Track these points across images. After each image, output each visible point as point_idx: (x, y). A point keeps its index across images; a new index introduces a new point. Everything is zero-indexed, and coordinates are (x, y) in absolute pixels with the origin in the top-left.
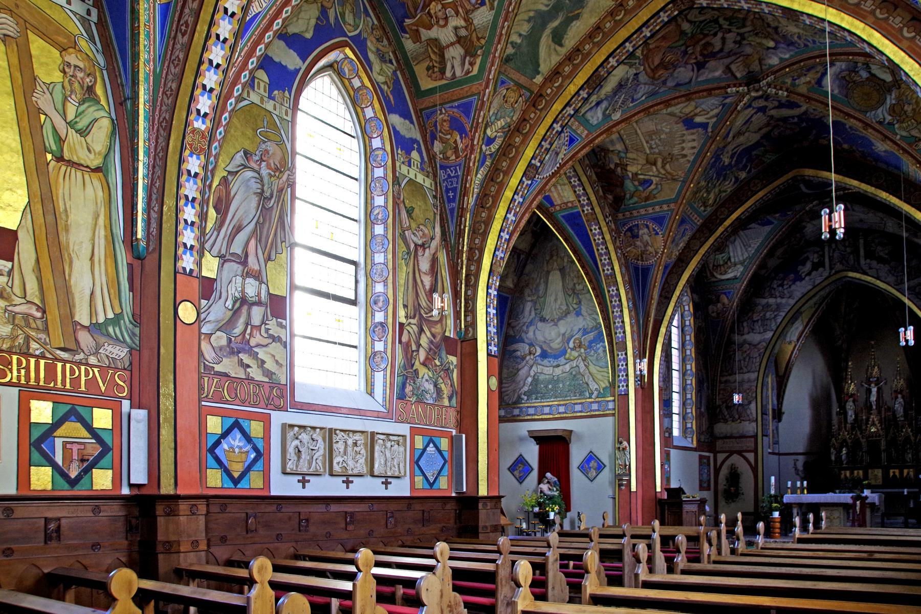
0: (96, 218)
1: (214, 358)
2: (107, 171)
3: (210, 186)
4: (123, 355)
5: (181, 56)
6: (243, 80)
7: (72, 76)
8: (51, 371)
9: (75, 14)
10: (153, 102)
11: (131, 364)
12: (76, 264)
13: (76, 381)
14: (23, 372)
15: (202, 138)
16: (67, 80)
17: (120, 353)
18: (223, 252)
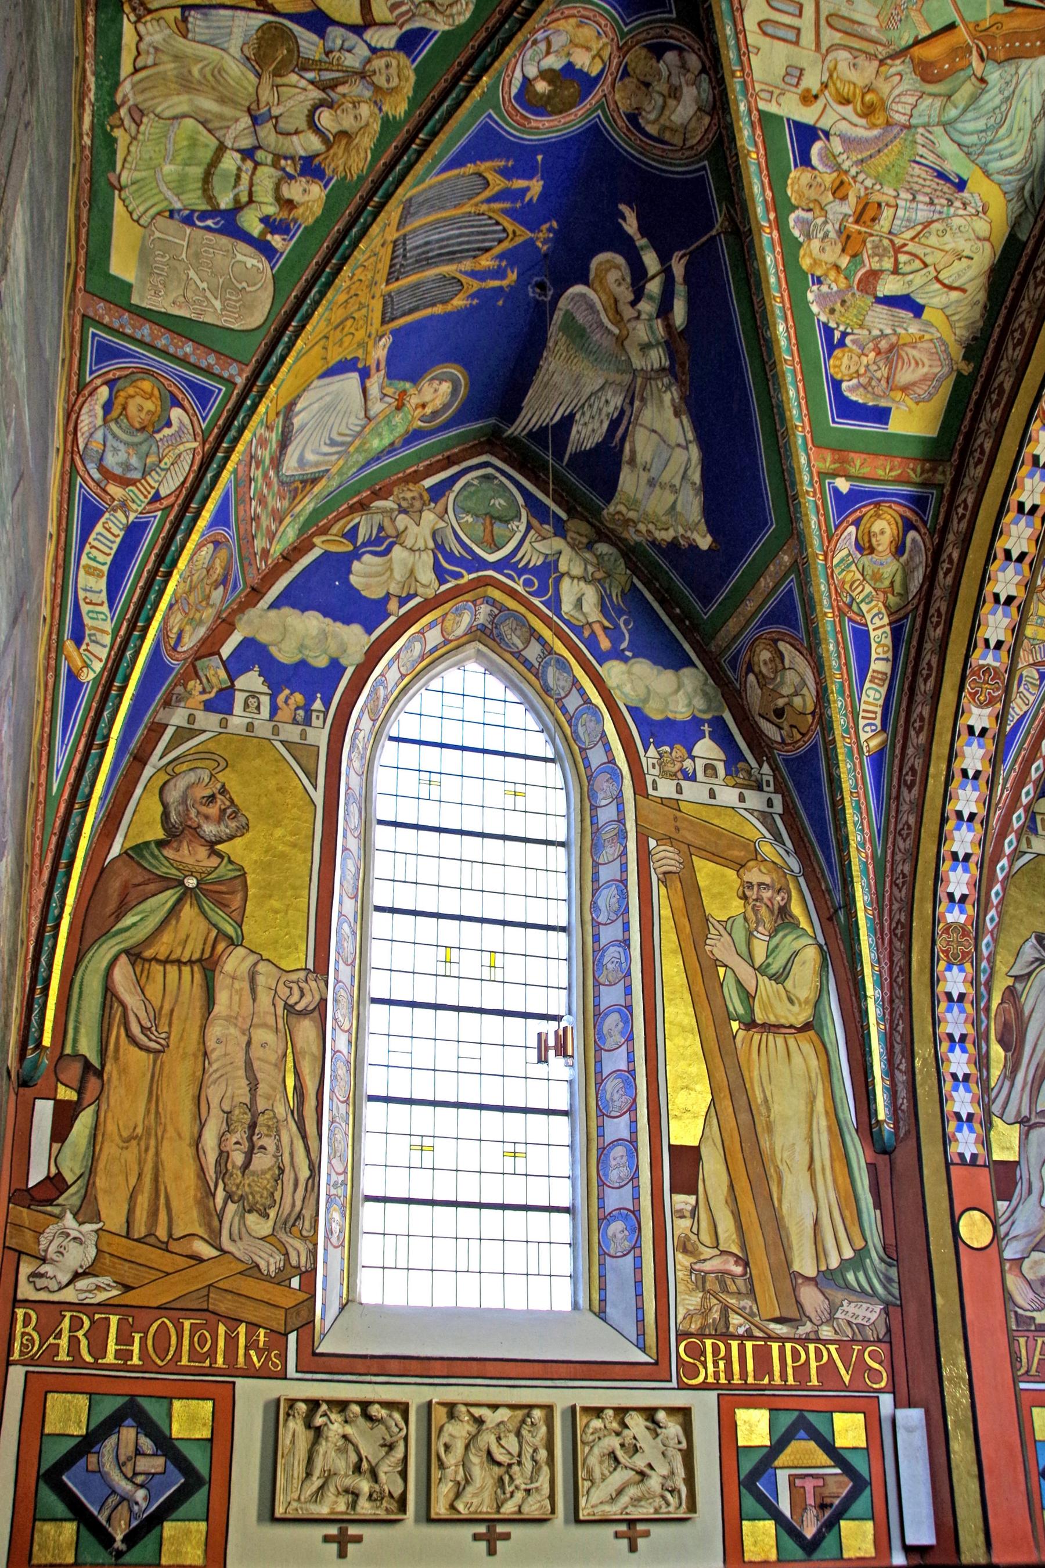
0: (812, 1100)
1: (1032, 1301)
2: (821, 1026)
3: (987, 1009)
4: (874, 1317)
5: (912, 820)
6: (1016, 825)
7: (756, 900)
8: (763, 1357)
9: (751, 811)
10: (878, 903)
11: (889, 1331)
12: (788, 1180)
13: (802, 1371)
14: (722, 1364)
15: (963, 935)
16: (749, 908)
17: (870, 1313)
18: (1025, 1112)
